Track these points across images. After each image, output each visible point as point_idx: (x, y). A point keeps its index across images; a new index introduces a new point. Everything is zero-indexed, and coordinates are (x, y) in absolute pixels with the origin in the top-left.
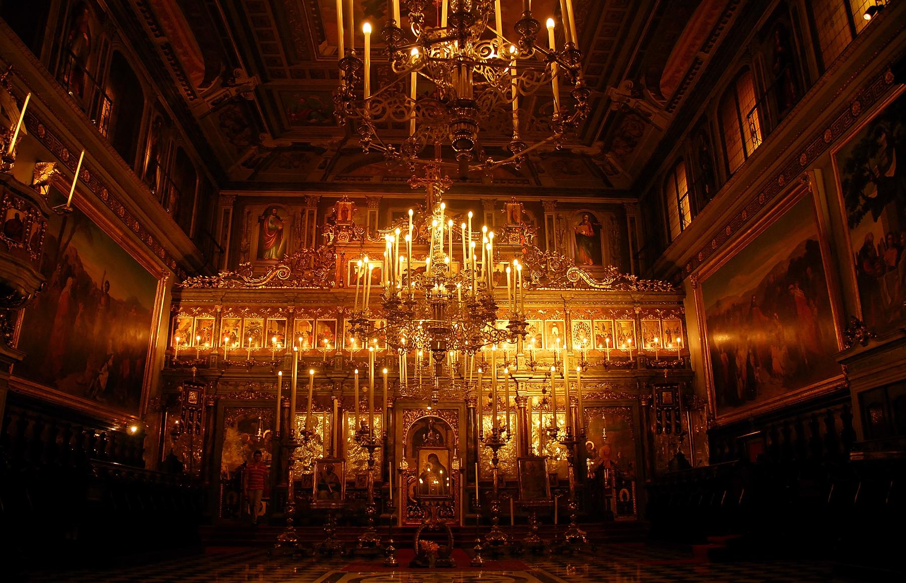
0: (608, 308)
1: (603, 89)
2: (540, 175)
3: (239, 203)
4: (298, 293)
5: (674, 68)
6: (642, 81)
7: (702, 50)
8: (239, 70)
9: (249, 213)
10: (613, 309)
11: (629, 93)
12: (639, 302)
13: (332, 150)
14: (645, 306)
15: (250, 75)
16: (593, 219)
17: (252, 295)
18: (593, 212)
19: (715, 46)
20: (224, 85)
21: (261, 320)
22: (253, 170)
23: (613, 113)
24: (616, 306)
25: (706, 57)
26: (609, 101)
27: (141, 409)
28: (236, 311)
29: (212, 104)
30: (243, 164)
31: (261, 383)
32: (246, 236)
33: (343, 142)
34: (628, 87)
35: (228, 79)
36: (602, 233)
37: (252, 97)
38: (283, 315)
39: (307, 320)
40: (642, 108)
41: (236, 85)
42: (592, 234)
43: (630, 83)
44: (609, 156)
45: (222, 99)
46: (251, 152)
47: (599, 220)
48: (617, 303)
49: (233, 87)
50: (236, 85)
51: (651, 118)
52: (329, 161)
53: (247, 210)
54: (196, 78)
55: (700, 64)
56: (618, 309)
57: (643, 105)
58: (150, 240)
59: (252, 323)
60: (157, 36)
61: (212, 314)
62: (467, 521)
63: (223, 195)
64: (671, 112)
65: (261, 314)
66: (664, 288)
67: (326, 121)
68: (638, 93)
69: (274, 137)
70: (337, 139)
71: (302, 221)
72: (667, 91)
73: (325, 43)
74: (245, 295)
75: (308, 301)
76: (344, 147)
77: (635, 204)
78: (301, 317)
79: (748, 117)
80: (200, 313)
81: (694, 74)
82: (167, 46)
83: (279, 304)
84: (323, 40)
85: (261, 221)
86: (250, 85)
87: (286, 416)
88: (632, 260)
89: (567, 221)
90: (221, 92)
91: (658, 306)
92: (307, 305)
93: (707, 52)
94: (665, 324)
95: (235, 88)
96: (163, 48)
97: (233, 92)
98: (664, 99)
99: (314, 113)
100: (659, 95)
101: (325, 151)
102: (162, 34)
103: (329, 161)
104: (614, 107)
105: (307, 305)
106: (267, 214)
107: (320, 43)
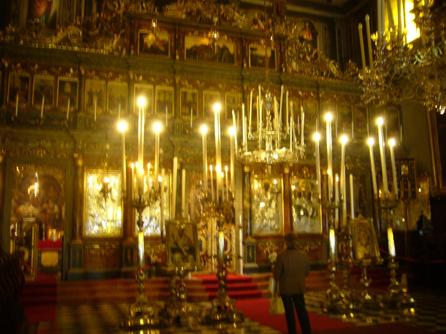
18: (313, 22)
21: (51, 78)
31: (53, 141)
62: (245, 270)
65: (51, 73)
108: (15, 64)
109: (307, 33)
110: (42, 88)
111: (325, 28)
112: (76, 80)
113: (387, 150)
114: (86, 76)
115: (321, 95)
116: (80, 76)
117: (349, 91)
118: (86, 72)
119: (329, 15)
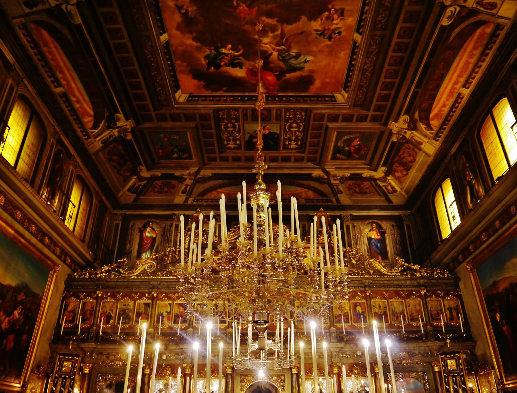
0: (399, 291)
1: (386, 124)
2: (339, 195)
3: (127, 219)
4: (162, 282)
5: (442, 102)
6: (416, 115)
7: (464, 86)
8: (118, 115)
9: (133, 226)
10: (403, 291)
11: (406, 126)
12: (423, 285)
13: (190, 179)
14: (428, 288)
15: (127, 119)
16: (379, 227)
17: (126, 284)
18: (379, 222)
19: (474, 82)
20: (109, 127)
21: (131, 302)
22: (135, 194)
23: (393, 143)
24: (405, 289)
25: (466, 92)
26: (391, 134)
27: (23, 377)
28: (113, 296)
29: (102, 143)
30: (129, 190)
32: (130, 243)
33: (198, 172)
34: (405, 121)
35: (111, 124)
36: (387, 237)
37: (129, 137)
38: (148, 298)
39: (167, 302)
40: (416, 138)
41: (118, 127)
42: (379, 237)
43: (406, 117)
44: (390, 179)
45: (108, 139)
46: (133, 181)
47: (384, 227)
48: (406, 286)
49: (115, 129)
50: (118, 127)
51: (422, 146)
52: (189, 187)
53: (131, 224)
54: (88, 121)
55: (462, 98)
56: (407, 291)
57: (417, 136)
58: (47, 240)
59: (125, 305)
60: (56, 87)
61: (94, 298)
63: (115, 214)
64: (437, 141)
65: (132, 298)
66: (440, 273)
67: (185, 156)
68: (413, 126)
69: (149, 169)
70: (193, 170)
71: (170, 231)
72: (435, 123)
73: (179, 92)
74: (120, 283)
75: (169, 288)
76: (199, 176)
77: (409, 215)
78: (162, 301)
79: (512, 127)
80: (85, 297)
81: (457, 107)
82: (64, 95)
83: (146, 290)
84: (178, 89)
85: (142, 231)
86: (128, 127)
87: (146, 381)
88: (410, 256)
89: (360, 229)
90: (106, 134)
91: (439, 288)
92: (167, 291)
93: (467, 88)
94: (446, 302)
95: (117, 130)
96: (61, 97)
97: (116, 132)
98: (432, 130)
99: (175, 149)
100: (429, 127)
101: (185, 179)
102: (60, 85)
103: (189, 187)
104: (394, 139)
105: (167, 291)
106: (145, 227)
107: (176, 92)
108: (107, 293)
109: (375, 232)
110: (124, 311)
111: (393, 226)
112: (150, 302)
113: (384, 351)
114: (157, 298)
115: (368, 294)
116: (153, 298)
117: (400, 286)
118: (157, 295)
119: (396, 213)
